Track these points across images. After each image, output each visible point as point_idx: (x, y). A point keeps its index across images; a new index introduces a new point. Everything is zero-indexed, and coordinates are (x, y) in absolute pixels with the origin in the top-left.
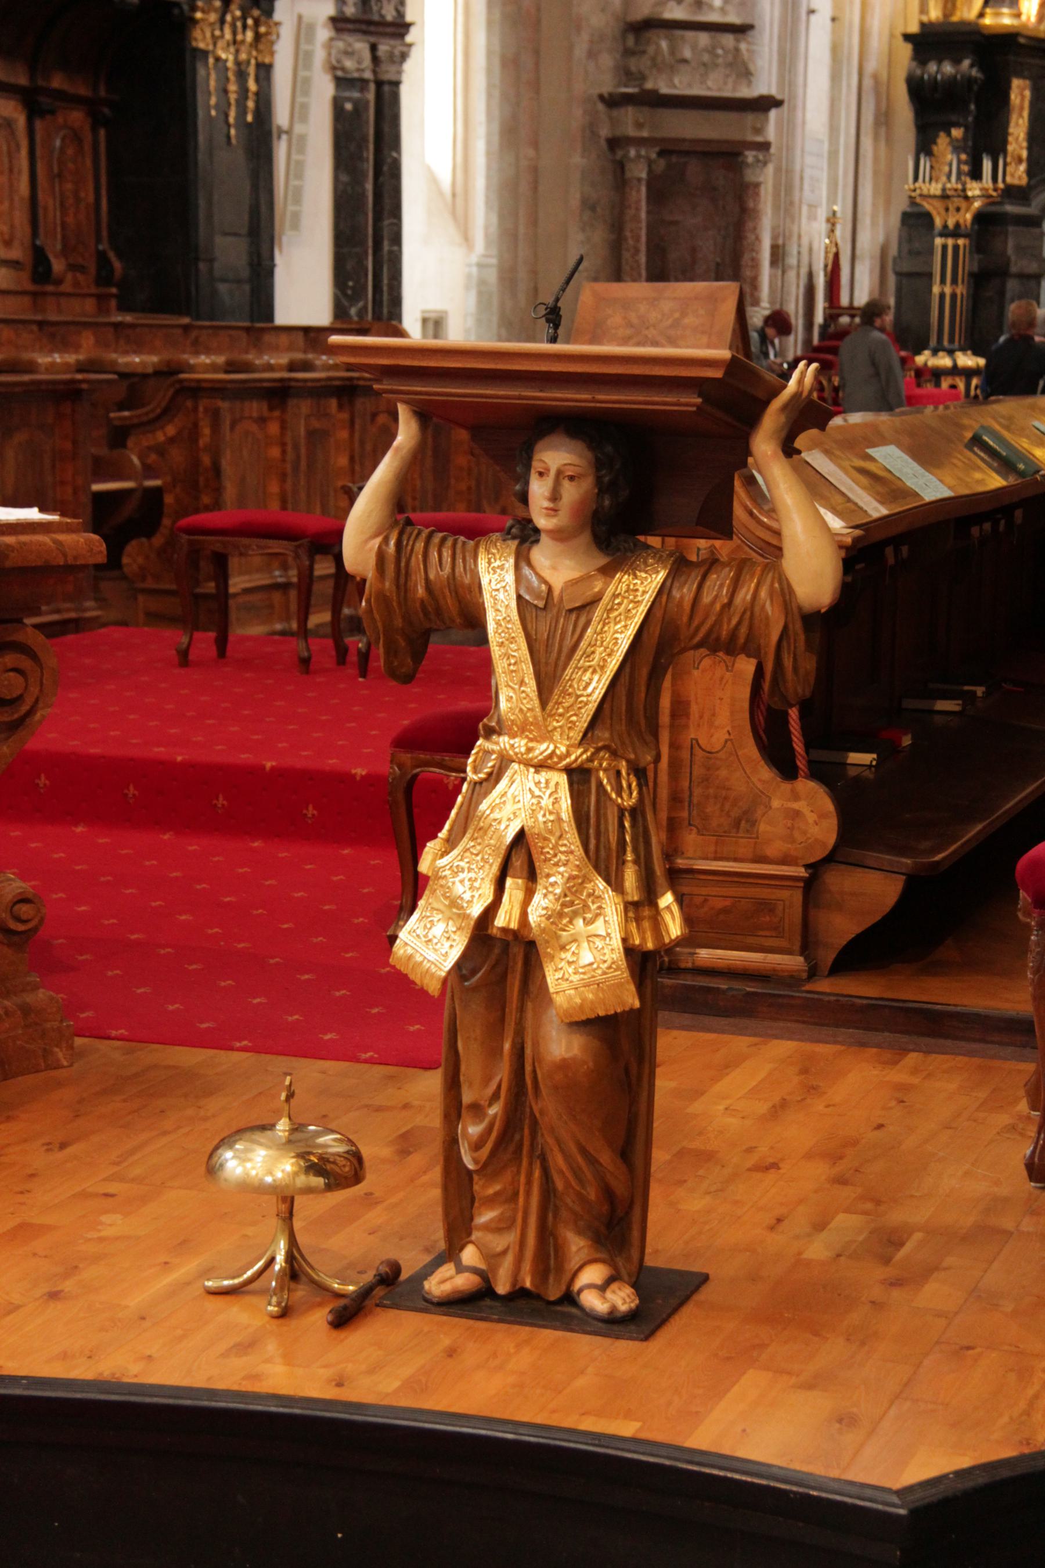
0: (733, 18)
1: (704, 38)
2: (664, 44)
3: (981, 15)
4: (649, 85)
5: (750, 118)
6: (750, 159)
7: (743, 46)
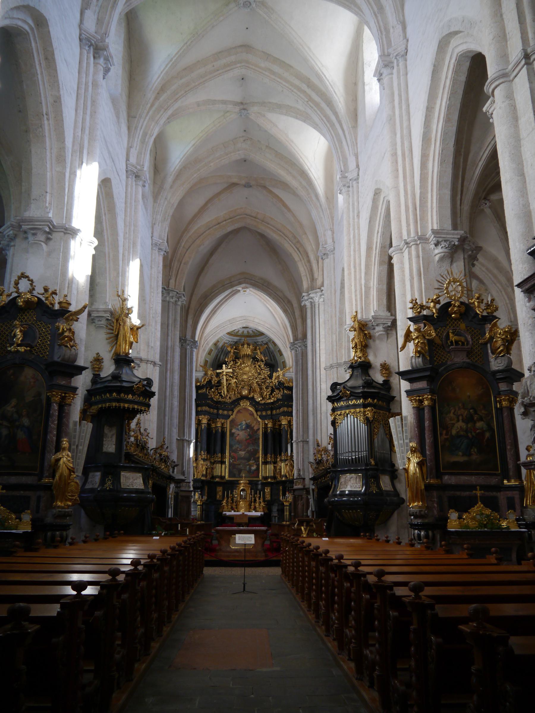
1: (185, 483)
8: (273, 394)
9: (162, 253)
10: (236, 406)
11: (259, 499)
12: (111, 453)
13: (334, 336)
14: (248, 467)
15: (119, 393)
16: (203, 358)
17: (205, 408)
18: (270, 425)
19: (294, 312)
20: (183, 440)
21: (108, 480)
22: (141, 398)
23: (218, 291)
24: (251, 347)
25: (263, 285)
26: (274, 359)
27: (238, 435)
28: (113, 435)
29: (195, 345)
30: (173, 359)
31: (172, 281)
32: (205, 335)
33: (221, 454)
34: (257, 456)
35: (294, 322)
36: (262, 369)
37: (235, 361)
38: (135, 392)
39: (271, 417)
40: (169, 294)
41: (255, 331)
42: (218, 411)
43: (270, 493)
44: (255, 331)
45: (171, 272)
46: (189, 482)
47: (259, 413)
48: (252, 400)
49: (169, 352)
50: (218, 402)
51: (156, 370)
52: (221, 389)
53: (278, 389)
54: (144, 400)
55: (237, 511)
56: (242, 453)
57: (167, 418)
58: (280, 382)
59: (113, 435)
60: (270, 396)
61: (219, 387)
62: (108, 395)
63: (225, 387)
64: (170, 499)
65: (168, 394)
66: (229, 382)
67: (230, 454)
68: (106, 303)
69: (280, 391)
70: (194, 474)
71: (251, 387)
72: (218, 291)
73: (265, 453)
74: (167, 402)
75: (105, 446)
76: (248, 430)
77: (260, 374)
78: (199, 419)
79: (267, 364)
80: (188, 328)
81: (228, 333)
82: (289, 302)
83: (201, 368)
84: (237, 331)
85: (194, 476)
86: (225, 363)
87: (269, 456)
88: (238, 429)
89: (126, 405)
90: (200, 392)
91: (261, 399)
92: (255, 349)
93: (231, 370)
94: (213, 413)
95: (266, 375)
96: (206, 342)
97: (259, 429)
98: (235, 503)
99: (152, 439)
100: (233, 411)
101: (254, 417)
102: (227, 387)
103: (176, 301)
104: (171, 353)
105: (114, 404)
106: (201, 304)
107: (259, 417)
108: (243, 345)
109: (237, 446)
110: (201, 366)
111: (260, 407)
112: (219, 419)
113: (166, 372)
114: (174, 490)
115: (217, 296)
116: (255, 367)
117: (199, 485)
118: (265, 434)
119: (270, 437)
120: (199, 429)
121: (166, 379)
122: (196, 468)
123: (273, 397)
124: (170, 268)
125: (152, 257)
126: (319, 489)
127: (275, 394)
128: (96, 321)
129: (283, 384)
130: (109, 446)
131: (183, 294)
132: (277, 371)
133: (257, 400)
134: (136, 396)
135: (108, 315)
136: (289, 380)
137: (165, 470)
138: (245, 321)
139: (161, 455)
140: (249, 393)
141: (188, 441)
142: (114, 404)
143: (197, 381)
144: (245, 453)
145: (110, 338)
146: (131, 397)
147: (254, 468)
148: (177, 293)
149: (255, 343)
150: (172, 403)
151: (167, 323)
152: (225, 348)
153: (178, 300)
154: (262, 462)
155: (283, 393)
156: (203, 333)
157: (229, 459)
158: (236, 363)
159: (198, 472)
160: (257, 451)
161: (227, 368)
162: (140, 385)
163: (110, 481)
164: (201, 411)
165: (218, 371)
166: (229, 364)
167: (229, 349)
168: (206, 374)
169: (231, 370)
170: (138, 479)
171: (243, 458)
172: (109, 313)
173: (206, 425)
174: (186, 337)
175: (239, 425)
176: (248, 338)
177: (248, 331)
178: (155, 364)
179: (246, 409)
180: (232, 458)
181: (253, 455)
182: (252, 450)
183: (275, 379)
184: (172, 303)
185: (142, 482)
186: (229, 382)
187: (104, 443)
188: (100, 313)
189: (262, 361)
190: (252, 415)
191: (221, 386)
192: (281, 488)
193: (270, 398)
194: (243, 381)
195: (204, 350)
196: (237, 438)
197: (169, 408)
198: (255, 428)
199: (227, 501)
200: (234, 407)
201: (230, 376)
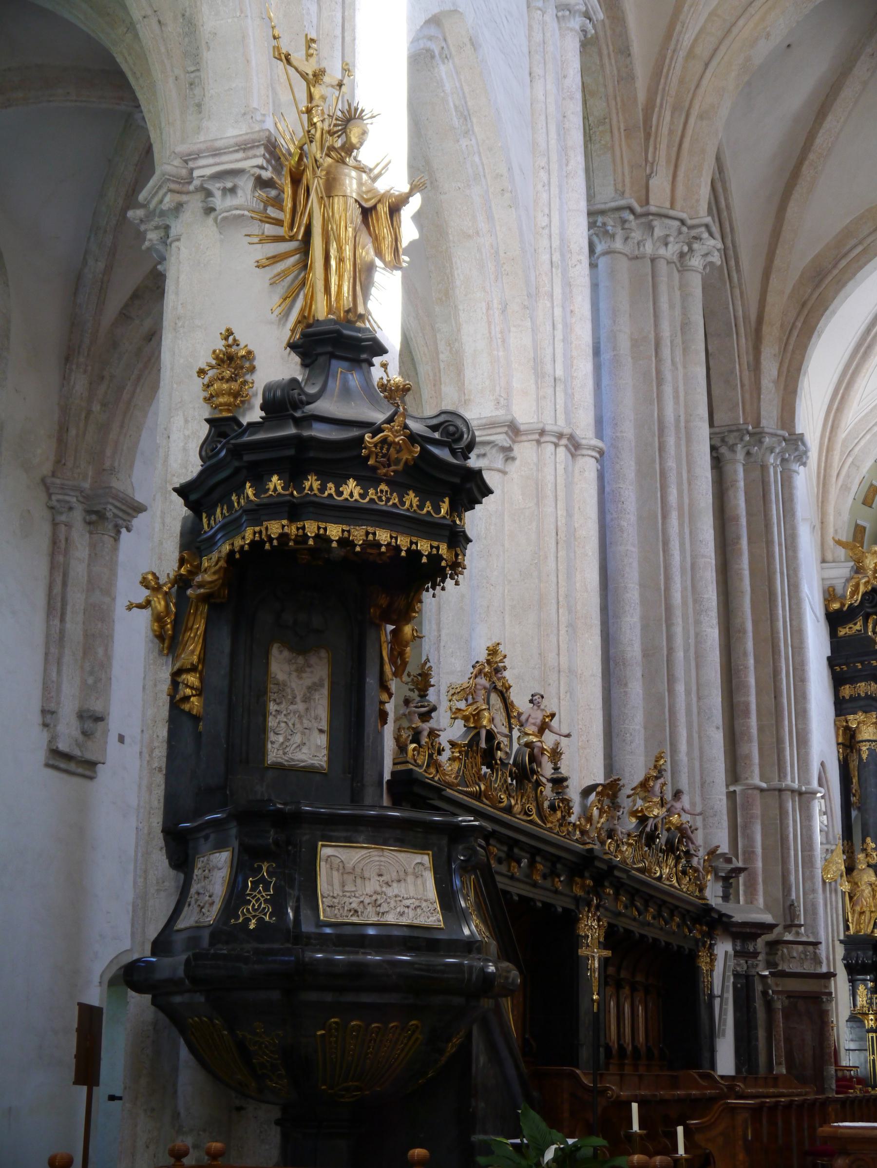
0: (811, 939)
1: (800, 948)
2: (785, 950)
3: (872, 932)
4: (780, 968)
5: (823, 981)
6: (825, 1000)
7: (817, 951)
9: (576, 23)
12: (309, 771)
15: (294, 477)
16: (846, 516)
17: (863, 688)
20: (780, 790)
21: (255, 885)
22: (412, 499)
23: (860, 249)
28: (313, 688)
29: (796, 449)
30: (689, 471)
31: (660, 184)
32: (842, 435)
38: (374, 469)
40: (651, 228)
45: (651, 149)
46: (816, 944)
49: (671, 441)
51: (582, 472)
54: (428, 507)
57: (680, 688)
59: (313, 688)
62: (250, 492)
64: (717, 1002)
68: (247, 113)
70: (846, 921)
72: (860, 249)
74: (678, 630)
75: (272, 737)
78: (847, 729)
80: (763, 391)
83: (841, 552)
85: (847, 928)
89: (334, 531)
90: (842, 632)
96: (850, 460)
99: (568, 736)
103: (682, 255)
104: (678, 446)
105: (275, 528)
106: (804, 304)
110: (839, 543)
113: (665, 517)
114: (731, 963)
115: (861, 268)
117: (866, 957)
120: (854, 764)
121: (666, 543)
122: (851, 898)
125: (530, 37)
128: (219, 202)
130: (297, 738)
131: (707, 226)
134: (383, 487)
135: (255, 161)
137: (685, 887)
139: (643, 820)
141: (801, 794)
142: (275, 528)
143: (829, 595)
145: (275, 259)
146: (357, 491)
148: (683, 222)
151: (652, 336)
153: (691, 250)
156: (834, 428)
159: (862, 913)
162: (396, 433)
163: (266, 889)
164: (852, 699)
168: (859, 569)
170: (410, 879)
172: (262, 151)
174: (757, 424)
178: (574, 446)
184: (668, 263)
185: (431, 892)
187: (272, 722)
188: (225, 158)
195: (845, 488)
197: (686, 651)
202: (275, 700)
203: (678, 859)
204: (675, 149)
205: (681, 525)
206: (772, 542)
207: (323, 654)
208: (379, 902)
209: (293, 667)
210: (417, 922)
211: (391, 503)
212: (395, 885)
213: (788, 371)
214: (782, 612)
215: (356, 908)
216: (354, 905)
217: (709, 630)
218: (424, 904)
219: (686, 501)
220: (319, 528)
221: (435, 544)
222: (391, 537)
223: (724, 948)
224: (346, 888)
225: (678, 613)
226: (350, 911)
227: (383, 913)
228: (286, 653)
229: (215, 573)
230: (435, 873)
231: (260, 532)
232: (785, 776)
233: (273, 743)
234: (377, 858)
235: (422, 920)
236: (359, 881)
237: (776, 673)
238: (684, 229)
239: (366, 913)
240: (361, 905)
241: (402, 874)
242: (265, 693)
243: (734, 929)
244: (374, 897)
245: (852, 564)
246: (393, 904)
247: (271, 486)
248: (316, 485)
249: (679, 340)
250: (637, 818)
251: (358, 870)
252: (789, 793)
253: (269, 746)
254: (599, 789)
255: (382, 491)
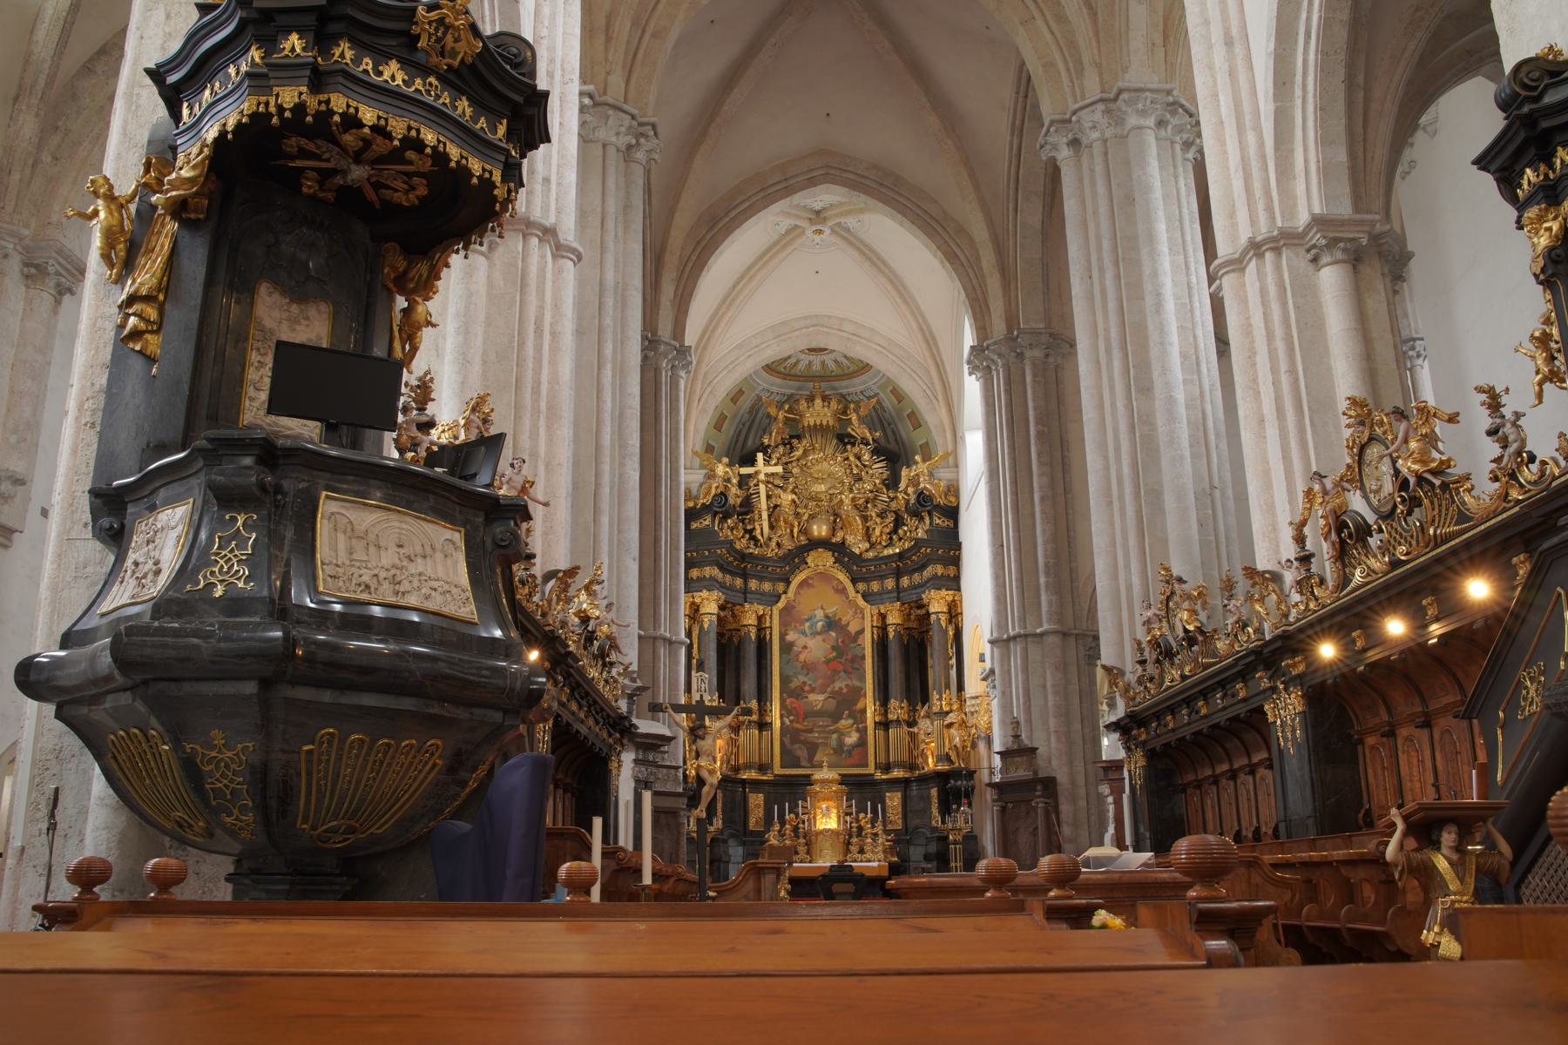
1: (665, 771)
8: (900, 531)
10: (795, 569)
11: (873, 827)
13: (1251, 138)
14: (835, 736)
15: (322, 40)
16: (701, 435)
18: (894, 618)
19: (978, 259)
20: (655, 638)
22: (464, 105)
23: (747, 204)
24: (834, 405)
25: (882, 184)
26: (896, 440)
27: (805, 647)
30: (622, 333)
33: (759, 701)
34: (860, 705)
35: (977, 286)
36: (865, 466)
37: (790, 444)
39: (895, 594)
41: (844, 361)
42: (746, 583)
43: (900, 810)
44: (845, 361)
47: (861, 586)
48: (840, 551)
49: (610, 302)
50: (743, 557)
52: (752, 521)
53: (916, 514)
55: (810, 862)
56: (817, 699)
57: (605, 520)
58: (922, 493)
60: (891, 539)
61: (747, 514)
63: (765, 515)
65: (607, 438)
66: (774, 501)
67: (783, 701)
69: (921, 519)
71: (836, 515)
72: (747, 204)
73: (883, 697)
75: (251, 392)
76: (833, 634)
77: (859, 479)
78: (693, 603)
79: (875, 452)
81: (769, 368)
82: (961, 230)
84: (793, 360)
86: (764, 449)
87: (893, 703)
88: (804, 633)
90: (694, 525)
91: (867, 545)
92: (844, 413)
93: (779, 469)
94: (731, 588)
95: (877, 481)
96: (709, 390)
97: (862, 631)
98: (805, 837)
100: (788, 582)
101: (847, 598)
102: (769, 516)
103: (629, 147)
107: (864, 596)
108: (811, 399)
109: (802, 678)
111: (864, 570)
112: (752, 603)
115: (747, 220)
116: (847, 459)
118: (881, 645)
119: (894, 652)
121: (599, 391)
123: (900, 539)
124: (608, 39)
126: (1151, 755)
127: (905, 532)
129: (930, 498)
131: (654, 126)
132: (909, 463)
133: (857, 551)
136: (945, 489)
138: (815, 328)
140: (833, 532)
141: (670, 642)
143: (688, 497)
144: (826, 699)
147: (852, 739)
148: (633, 117)
149: (843, 396)
150: (621, 476)
151: (599, 209)
152: (760, 415)
153: (638, 144)
154: (875, 723)
155: (931, 524)
157: (782, 716)
158: (792, 449)
160: (858, 693)
161: (767, 462)
165: (745, 470)
166: (773, 452)
167: (772, 411)
168: (711, 476)
169: (779, 469)
170: (439, 556)
171: (820, 714)
173: (714, 618)
174: (654, 333)
175: (807, 620)
176: (823, 384)
177: (823, 363)
179: (825, 577)
180: (790, 713)
181: (847, 703)
182: (845, 691)
183: (907, 487)
184: (618, 150)
185: (463, 578)
186: (774, 501)
189: (865, 442)
190: (843, 591)
191: (753, 512)
192: (934, 792)
193: (890, 544)
194: (812, 499)
196: (802, 658)
198: (853, 628)
199: (779, 831)
200: (792, 572)
201: (778, 486)
202: (258, 349)
203: (604, 665)
204: (631, 57)
205: (614, 376)
206: (661, 431)
207: (323, 307)
208: (398, 579)
209: (285, 315)
210: (446, 610)
211: (441, 101)
212: (419, 560)
213: (682, 295)
214: (664, 491)
215: (393, 549)
216: (365, 578)
217: (632, 472)
218: (454, 591)
219: (619, 358)
220: (348, 106)
221: (488, 167)
222: (439, 141)
223: (628, 757)
224: (355, 556)
225: (607, 453)
226: (360, 585)
227: (403, 593)
228: (276, 296)
229: (194, 167)
230: (468, 557)
231: (267, 104)
232: (660, 627)
233: (252, 399)
234: (396, 524)
235: (451, 609)
236: (372, 549)
237: (656, 541)
238: (635, 123)
239: (381, 589)
240: (375, 578)
241: (428, 549)
242: (247, 339)
243: (639, 740)
244: (393, 572)
245: (706, 471)
246: (416, 584)
247: (288, 45)
248: (349, 54)
249: (621, 218)
250: (580, 617)
251: (372, 537)
252: (662, 641)
253: (247, 403)
254: (561, 575)
255: (431, 84)
